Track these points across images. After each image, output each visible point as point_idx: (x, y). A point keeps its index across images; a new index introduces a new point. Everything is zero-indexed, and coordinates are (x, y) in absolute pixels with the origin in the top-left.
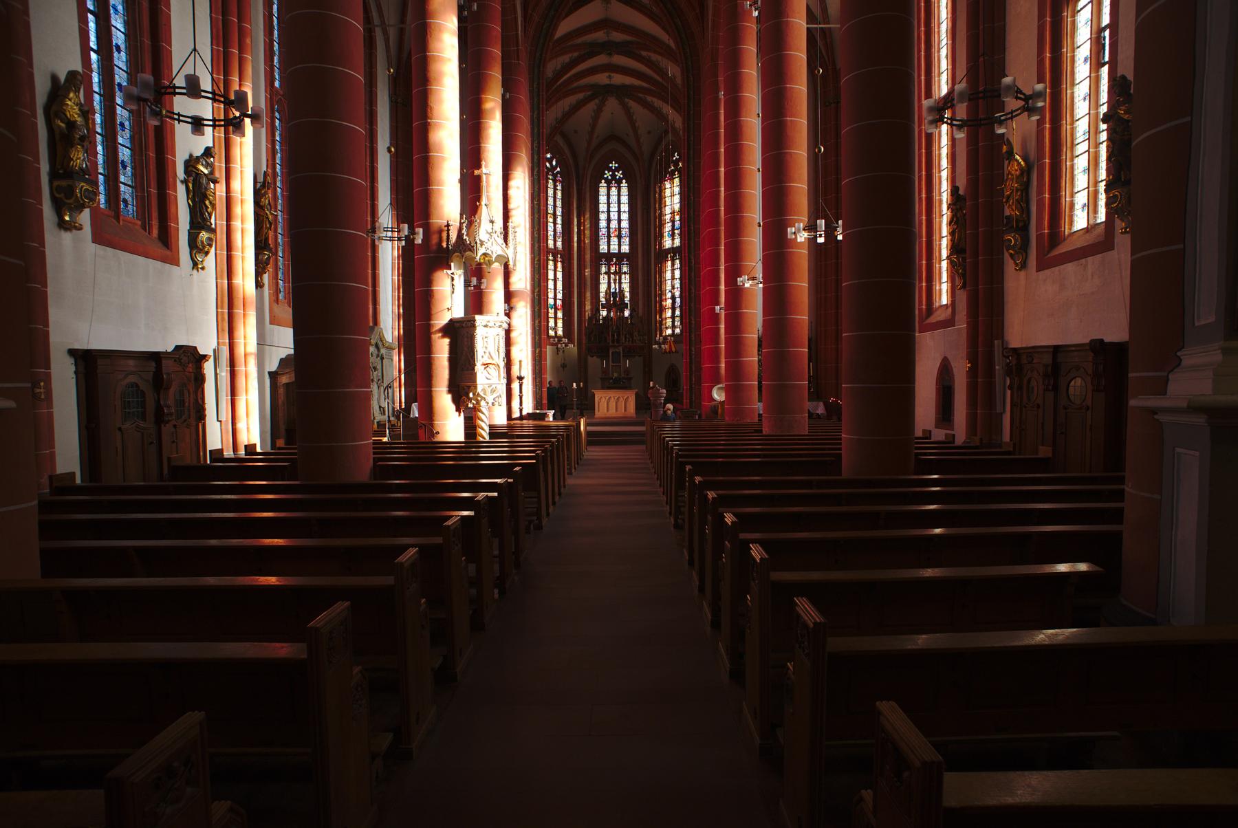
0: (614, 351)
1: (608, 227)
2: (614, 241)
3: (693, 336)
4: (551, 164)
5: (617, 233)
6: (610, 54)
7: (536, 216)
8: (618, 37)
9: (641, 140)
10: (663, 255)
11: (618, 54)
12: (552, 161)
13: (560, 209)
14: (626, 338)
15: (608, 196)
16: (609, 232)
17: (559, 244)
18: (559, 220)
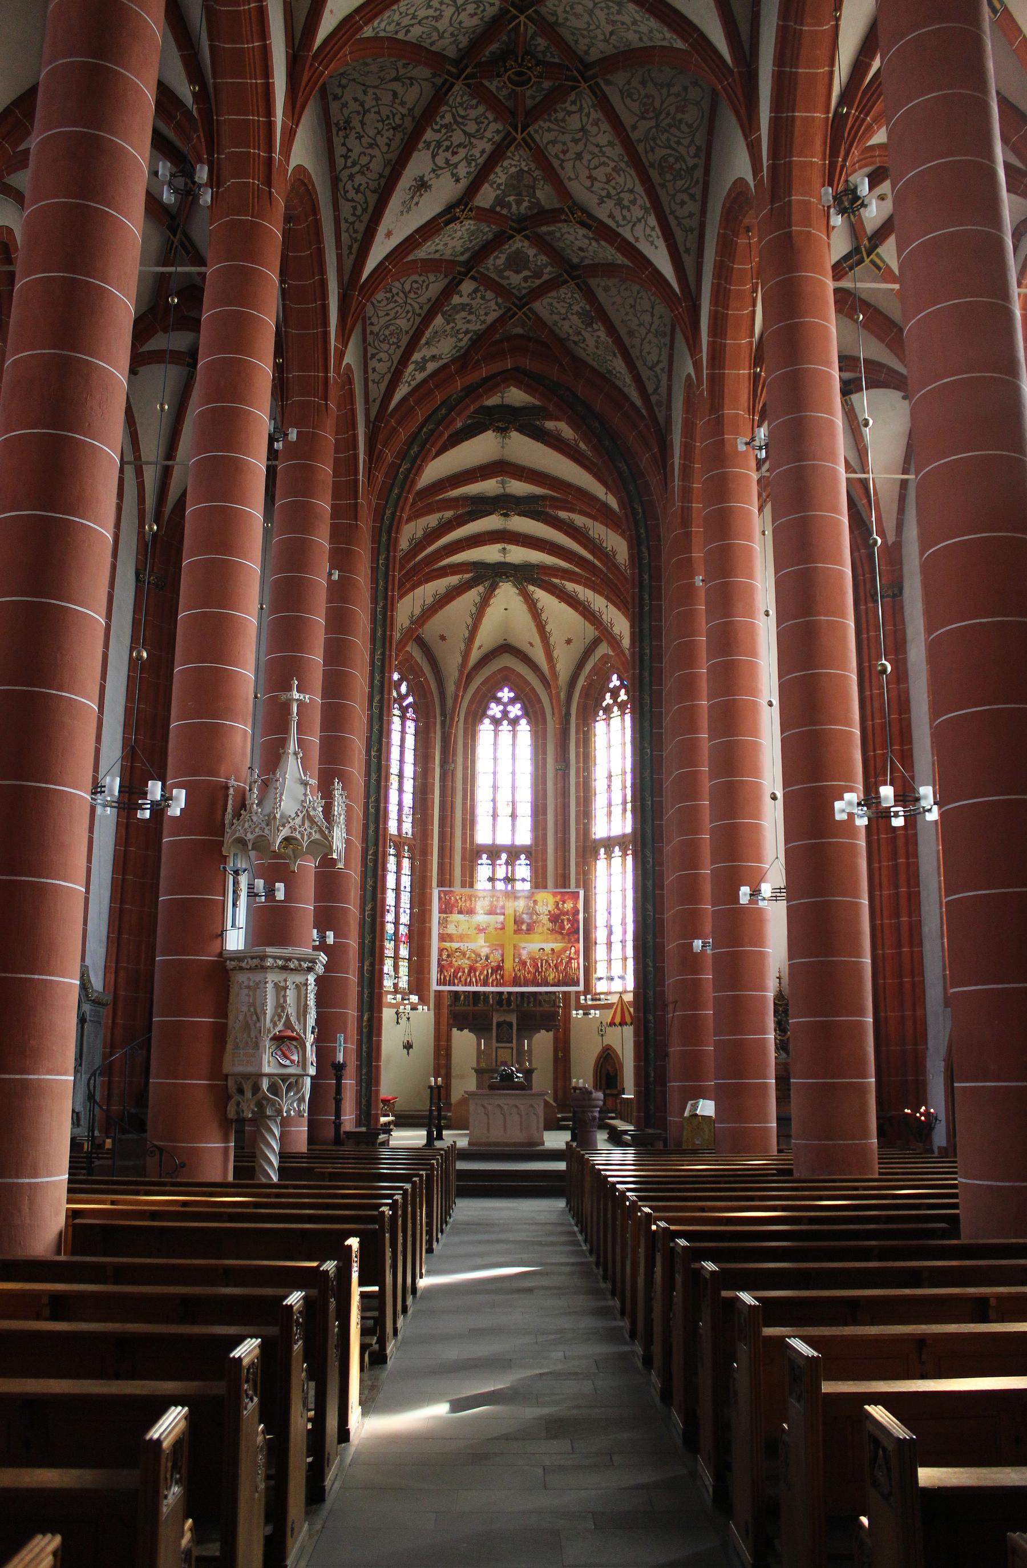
0: (501, 1019)
2: (504, 822)
3: (651, 993)
6: (505, 515)
7: (374, 776)
8: (518, 488)
9: (555, 654)
10: (589, 849)
11: (519, 515)
12: (400, 685)
17: (407, 827)
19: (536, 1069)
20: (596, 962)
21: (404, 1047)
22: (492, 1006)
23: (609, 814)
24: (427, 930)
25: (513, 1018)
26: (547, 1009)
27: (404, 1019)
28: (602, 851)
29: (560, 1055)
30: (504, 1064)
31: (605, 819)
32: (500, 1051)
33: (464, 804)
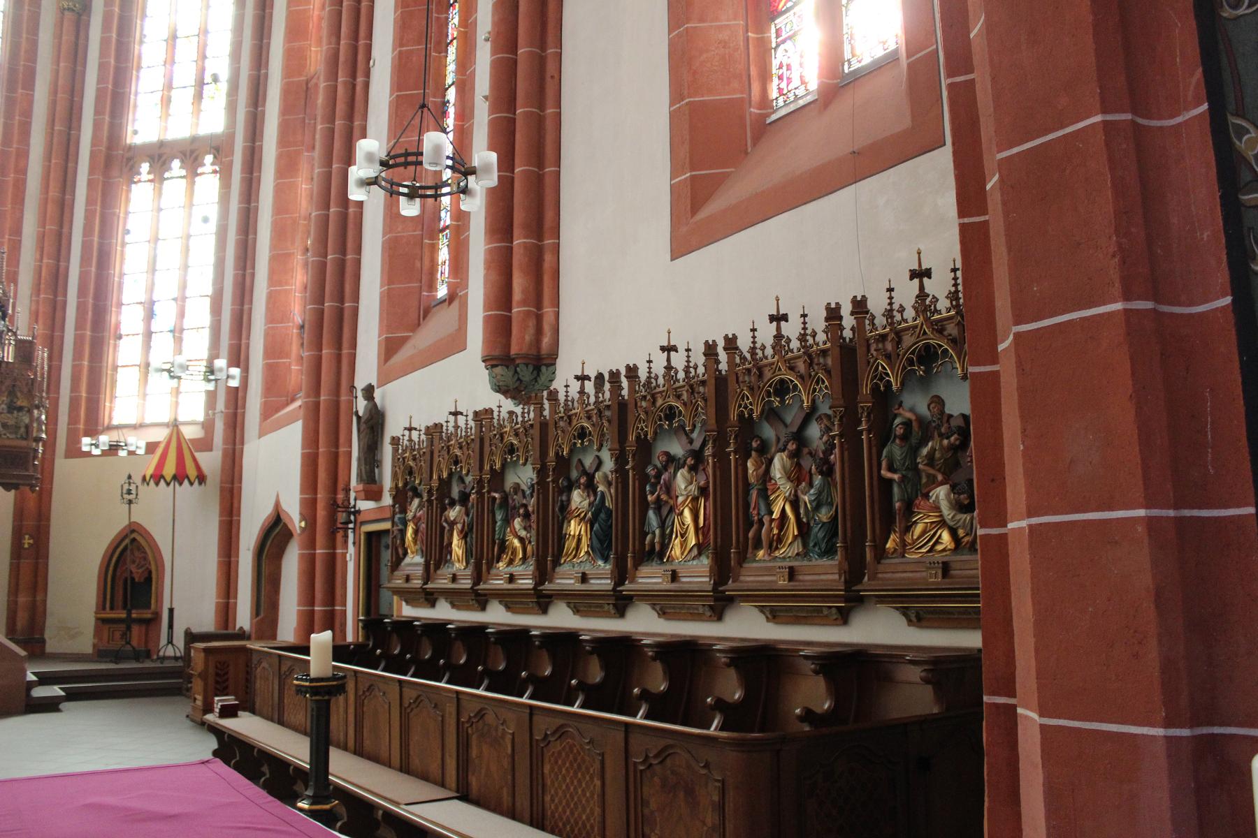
20: (115, 368)
23: (166, 102)
26: (7, 443)
28: (145, 167)
29: (27, 541)
31: (157, 110)
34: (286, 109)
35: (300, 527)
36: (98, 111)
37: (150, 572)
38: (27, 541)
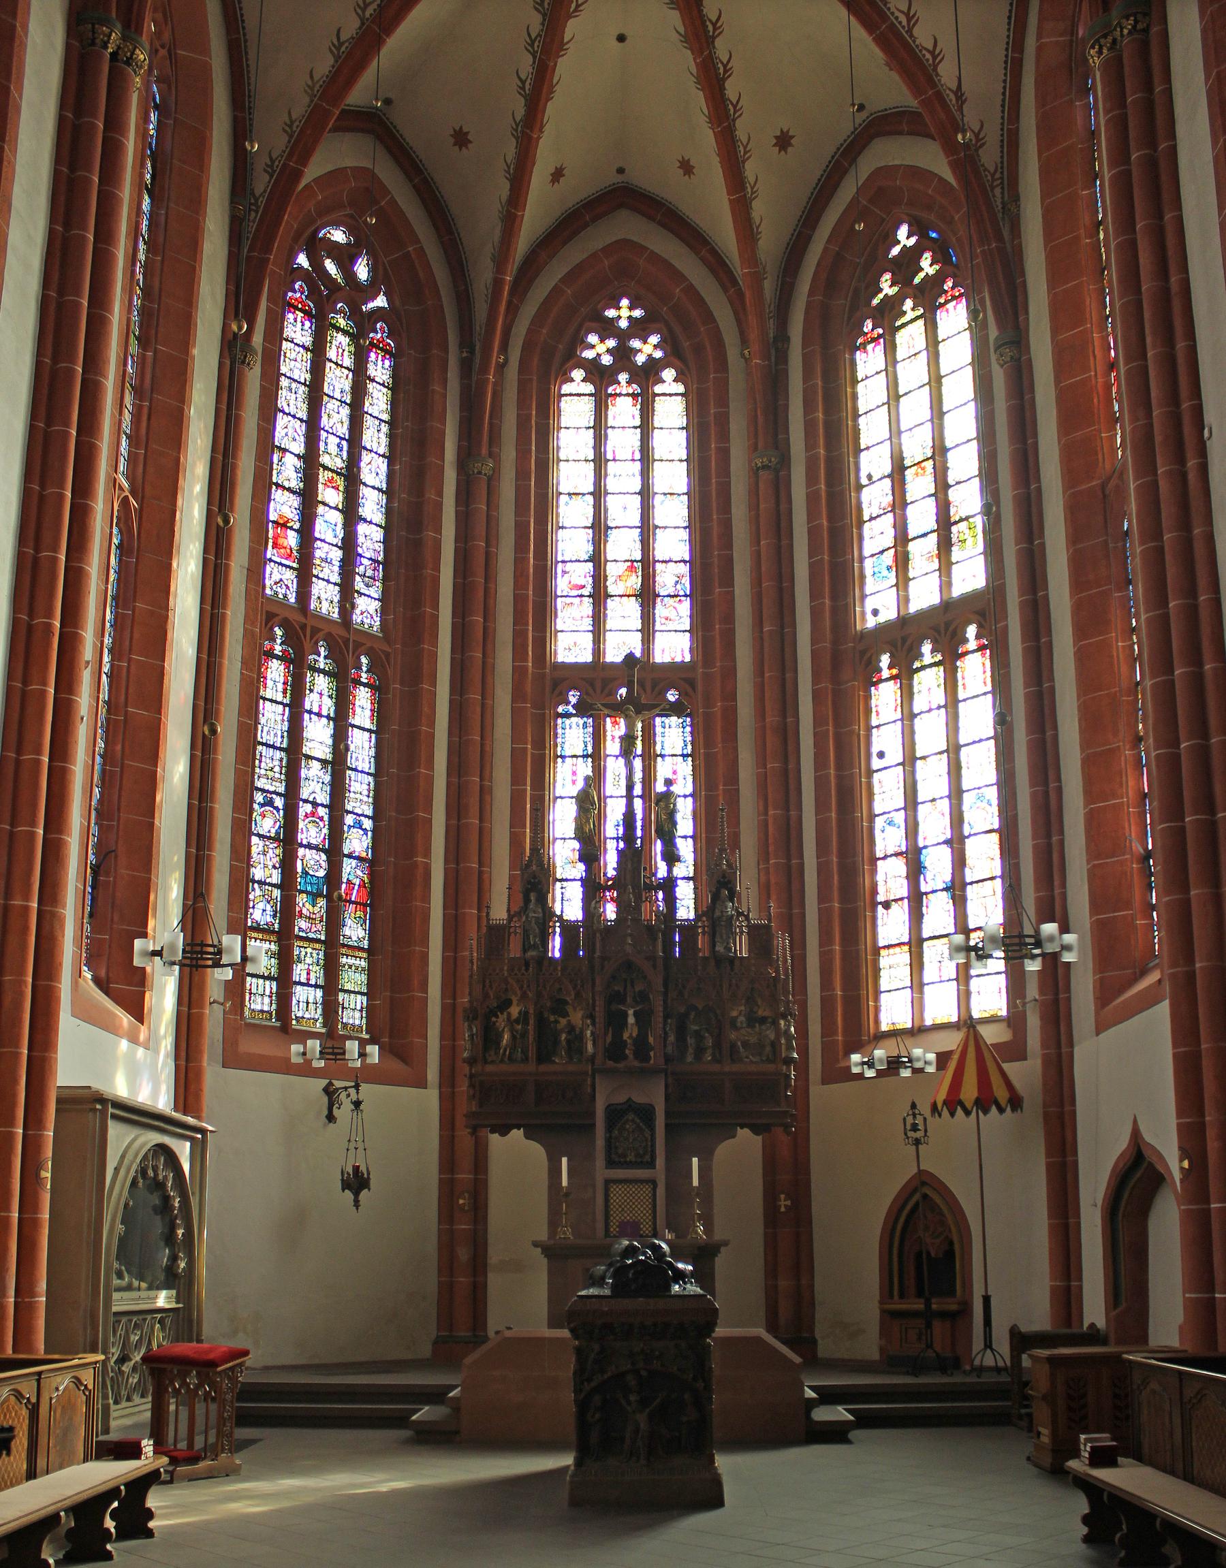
0: (621, 1098)
1: (597, 559)
4: (346, 266)
5: (635, 582)
13: (383, 465)
14: (681, 1031)
15: (600, 428)
16: (599, 578)
17: (367, 609)
18: (372, 505)
19: (726, 1243)
21: (346, 1185)
22: (592, 1059)
24: (420, 871)
25: (655, 1095)
26: (753, 1068)
27: (347, 1106)
30: (631, 1229)
32: (614, 1188)
33: (520, 561)
34: (1076, 534)
35: (1182, 1169)
36: (815, 594)
37: (951, 1243)
38: (784, 1203)
